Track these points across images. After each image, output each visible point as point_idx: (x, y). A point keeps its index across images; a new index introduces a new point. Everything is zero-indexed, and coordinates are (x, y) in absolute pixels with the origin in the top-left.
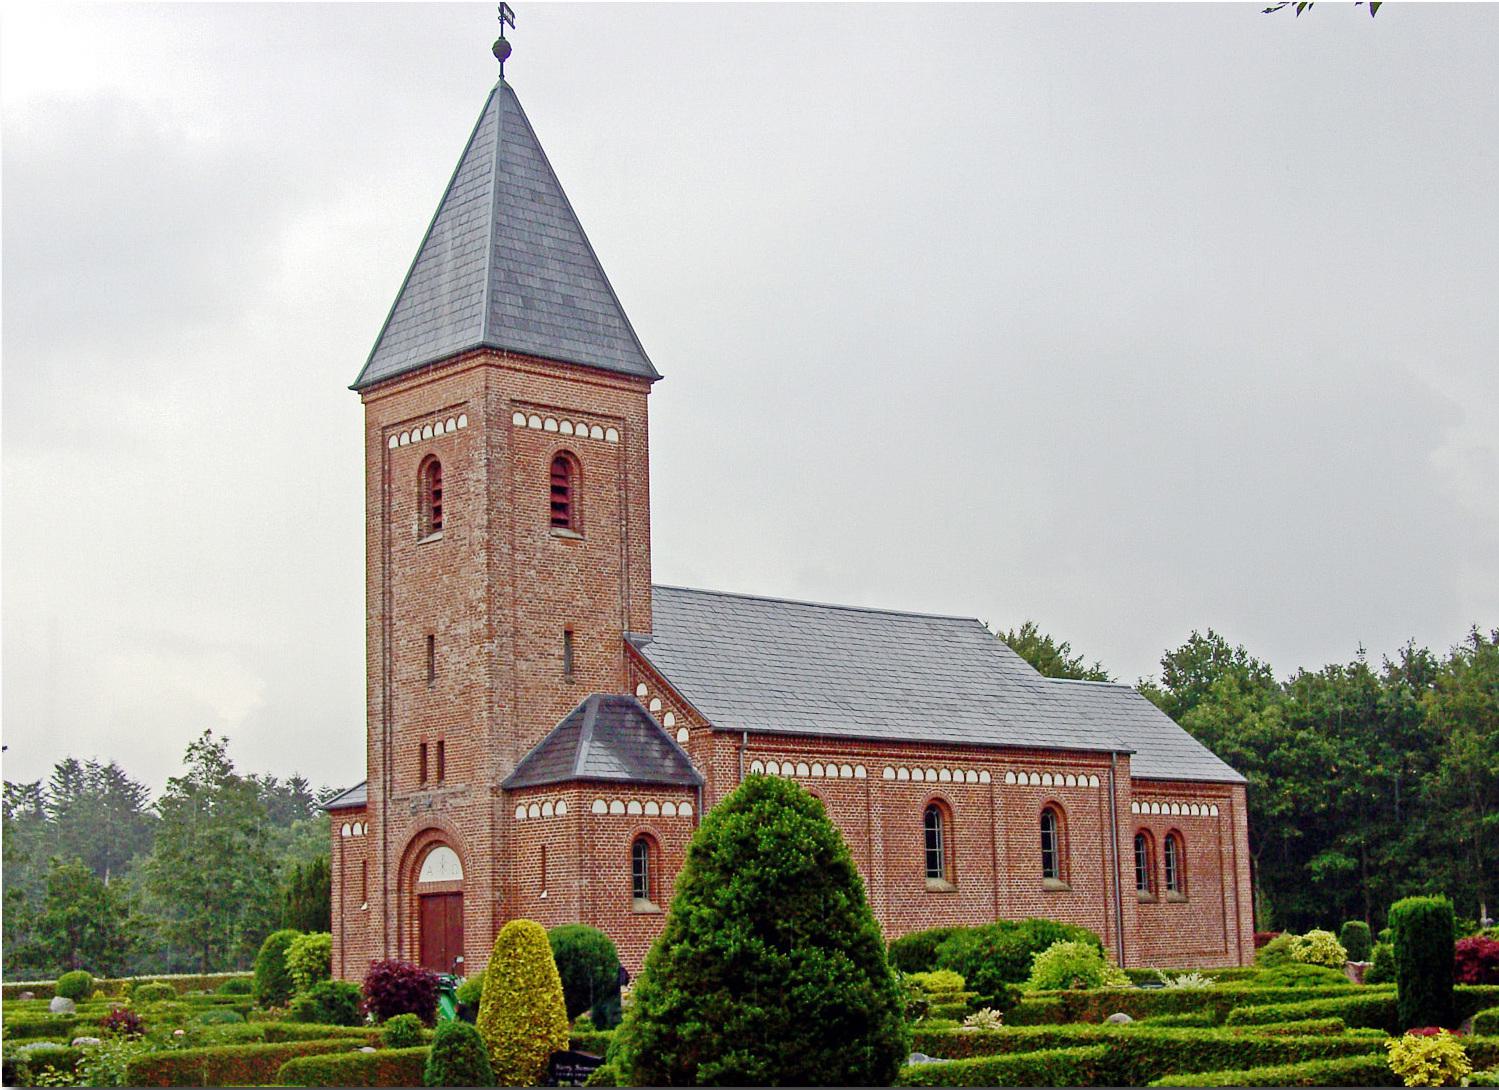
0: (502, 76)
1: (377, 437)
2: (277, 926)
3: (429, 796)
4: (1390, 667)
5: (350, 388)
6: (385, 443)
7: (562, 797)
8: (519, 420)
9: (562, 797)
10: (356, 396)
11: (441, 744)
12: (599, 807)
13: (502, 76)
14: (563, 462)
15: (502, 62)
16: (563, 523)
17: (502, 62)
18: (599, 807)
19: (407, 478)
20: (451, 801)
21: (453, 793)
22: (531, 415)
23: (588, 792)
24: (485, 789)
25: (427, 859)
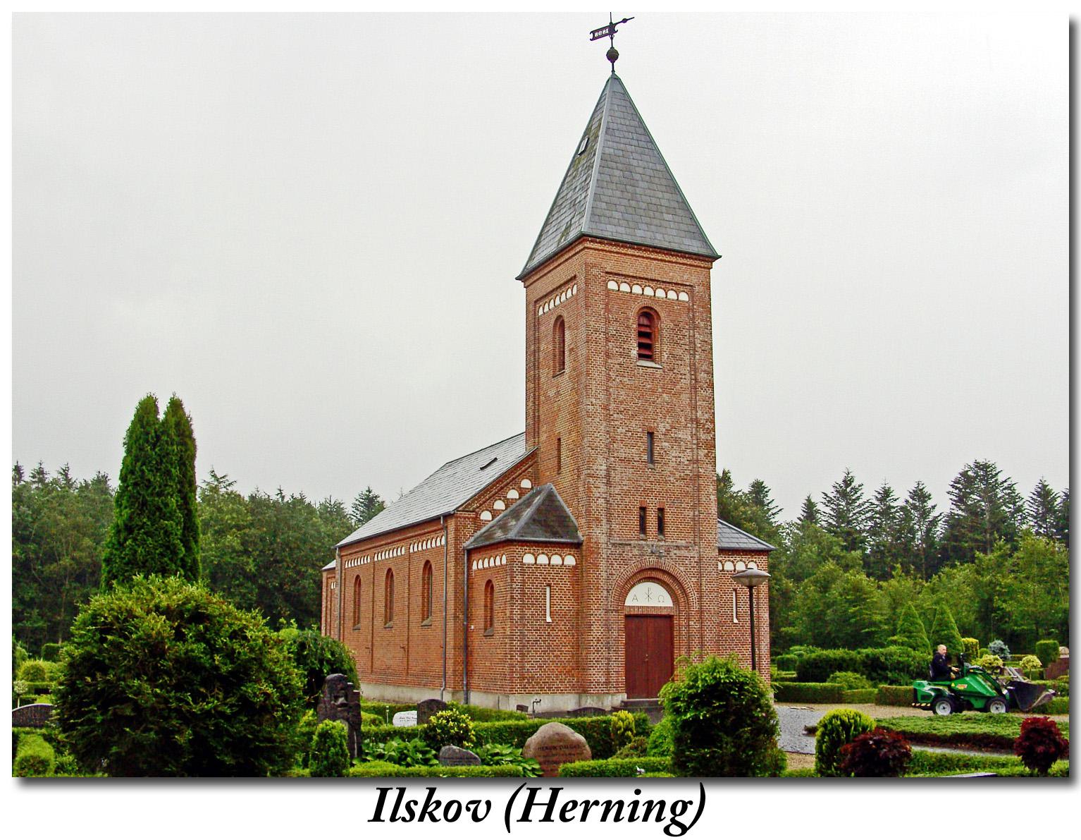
0: (613, 71)
1: (533, 304)
2: (1049, 635)
3: (653, 546)
4: (886, 494)
5: (517, 279)
6: (535, 312)
7: (754, 560)
8: (612, 285)
9: (754, 560)
10: (521, 284)
11: (661, 510)
12: (528, 559)
13: (613, 71)
14: (648, 314)
15: (613, 63)
16: (649, 358)
17: (613, 63)
18: (528, 559)
19: (547, 328)
20: (675, 552)
21: (677, 546)
22: (622, 282)
23: (519, 549)
24: (713, 548)
25: (664, 590)
